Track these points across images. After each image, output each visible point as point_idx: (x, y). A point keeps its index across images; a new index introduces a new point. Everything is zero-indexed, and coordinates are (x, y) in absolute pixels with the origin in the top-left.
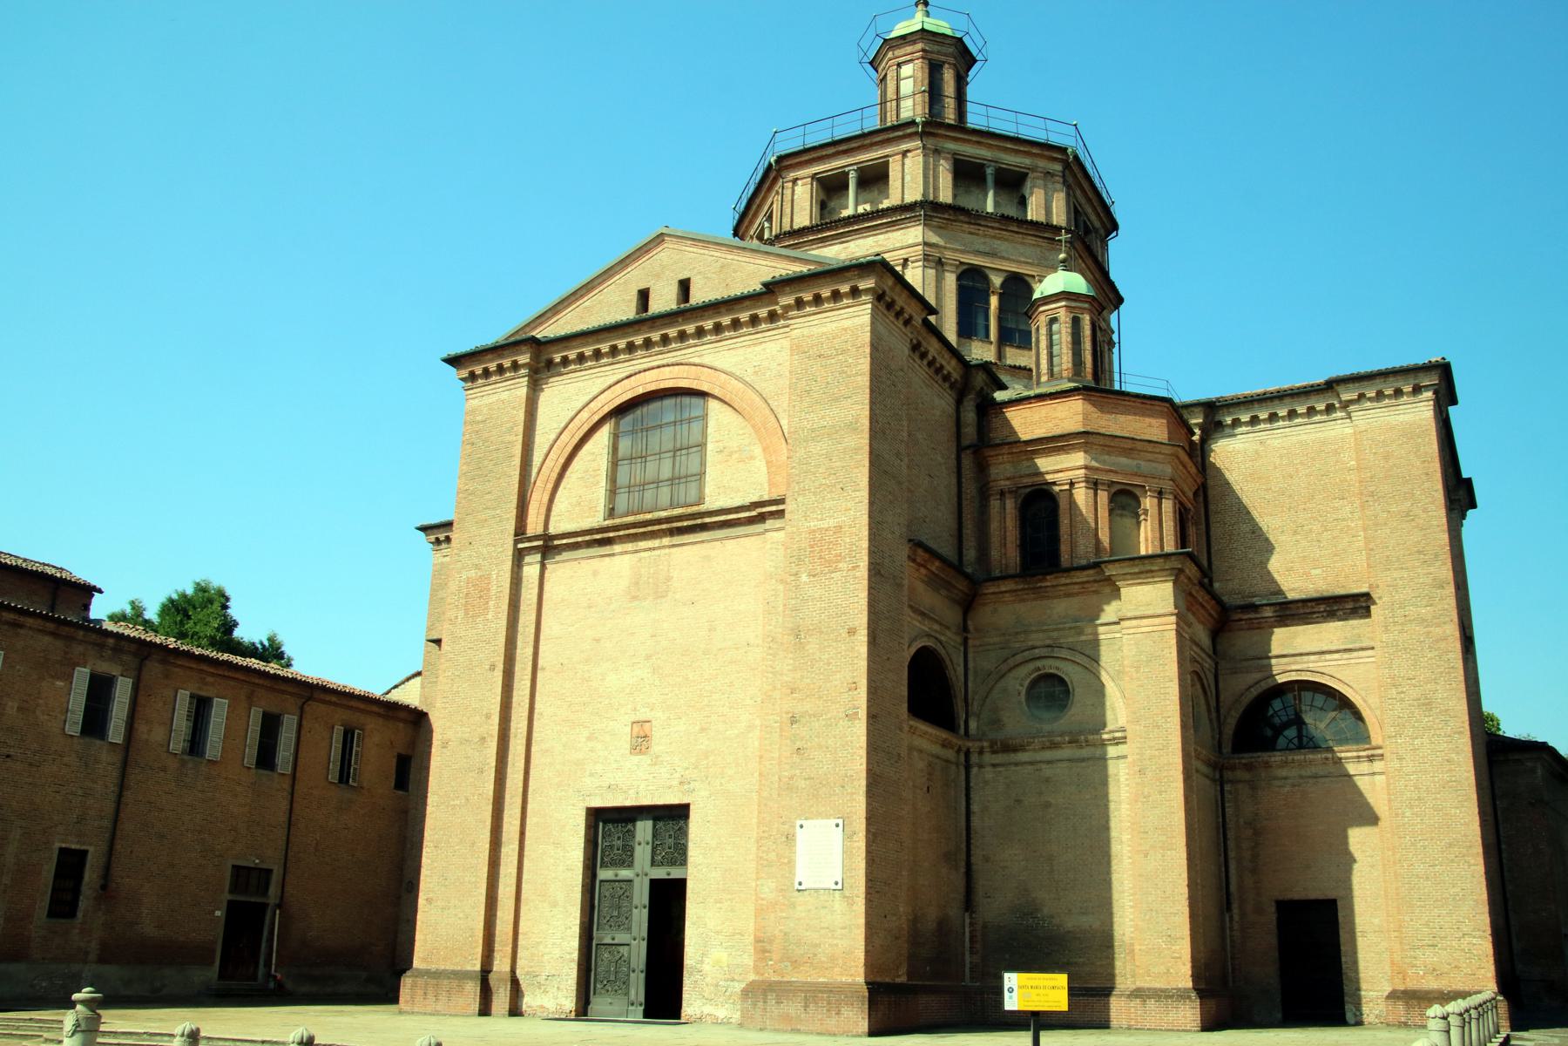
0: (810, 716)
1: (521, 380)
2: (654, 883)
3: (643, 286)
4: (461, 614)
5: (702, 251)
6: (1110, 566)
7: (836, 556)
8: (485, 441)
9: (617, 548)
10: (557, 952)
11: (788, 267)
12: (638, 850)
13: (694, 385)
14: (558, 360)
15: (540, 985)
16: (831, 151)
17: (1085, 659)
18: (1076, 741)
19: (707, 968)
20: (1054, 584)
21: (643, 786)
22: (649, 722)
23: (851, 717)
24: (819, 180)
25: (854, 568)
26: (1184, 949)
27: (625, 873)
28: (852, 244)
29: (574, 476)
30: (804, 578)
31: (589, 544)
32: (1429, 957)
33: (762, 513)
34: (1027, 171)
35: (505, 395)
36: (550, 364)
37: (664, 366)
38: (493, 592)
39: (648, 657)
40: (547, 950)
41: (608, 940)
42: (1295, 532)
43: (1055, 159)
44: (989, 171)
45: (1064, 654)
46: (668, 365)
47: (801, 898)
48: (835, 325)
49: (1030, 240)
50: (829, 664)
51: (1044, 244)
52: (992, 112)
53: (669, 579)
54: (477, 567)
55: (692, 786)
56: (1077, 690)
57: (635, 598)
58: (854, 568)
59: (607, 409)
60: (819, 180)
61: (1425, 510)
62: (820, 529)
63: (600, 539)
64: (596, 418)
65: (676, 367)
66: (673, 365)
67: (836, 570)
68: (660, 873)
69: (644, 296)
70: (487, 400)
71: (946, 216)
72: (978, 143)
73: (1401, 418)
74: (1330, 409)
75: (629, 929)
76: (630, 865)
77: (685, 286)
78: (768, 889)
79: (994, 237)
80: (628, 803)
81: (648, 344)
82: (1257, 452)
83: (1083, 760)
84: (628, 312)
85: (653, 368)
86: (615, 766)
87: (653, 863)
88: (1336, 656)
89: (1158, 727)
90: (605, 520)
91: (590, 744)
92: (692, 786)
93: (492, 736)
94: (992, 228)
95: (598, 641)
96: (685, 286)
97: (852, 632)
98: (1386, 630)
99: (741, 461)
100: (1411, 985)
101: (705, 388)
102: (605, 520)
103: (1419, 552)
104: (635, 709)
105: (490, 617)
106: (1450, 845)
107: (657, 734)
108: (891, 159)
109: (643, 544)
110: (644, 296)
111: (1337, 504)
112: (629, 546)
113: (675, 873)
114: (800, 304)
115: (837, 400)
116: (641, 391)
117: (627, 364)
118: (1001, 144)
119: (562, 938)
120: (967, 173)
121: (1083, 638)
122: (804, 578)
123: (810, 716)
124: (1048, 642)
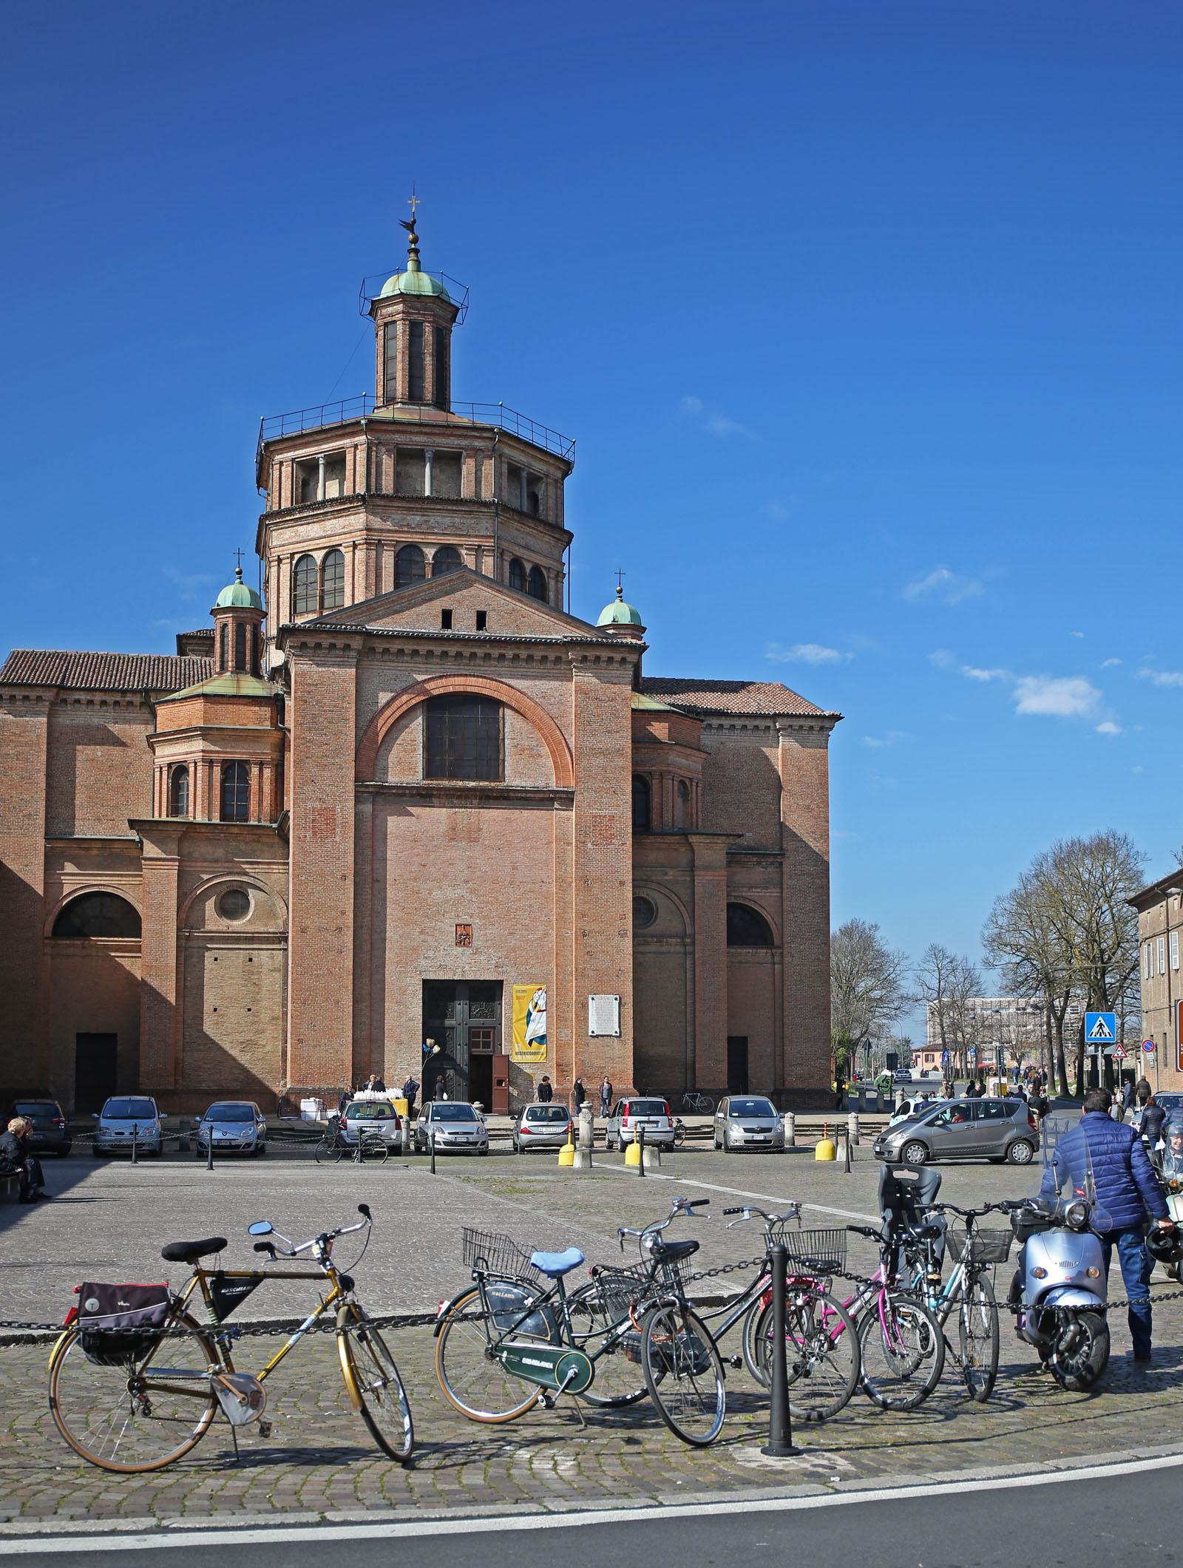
0: (596, 932)
1: (350, 660)
4: (309, 834)
5: (496, 594)
6: (693, 837)
7: (611, 834)
9: (435, 801)
11: (577, 631)
13: (495, 695)
14: (381, 650)
16: (416, 429)
17: (667, 891)
18: (661, 942)
20: (653, 841)
22: (469, 925)
24: (398, 449)
25: (623, 844)
26: (724, 1067)
30: (589, 845)
31: (412, 796)
34: (542, 476)
36: (373, 650)
37: (470, 675)
40: (397, 1073)
42: (738, 807)
43: (559, 468)
44: (524, 474)
45: (654, 886)
46: (474, 676)
47: (593, 1041)
50: (607, 902)
52: (536, 428)
55: (504, 969)
56: (660, 910)
58: (623, 844)
60: (398, 449)
61: (818, 807)
62: (600, 816)
63: (423, 796)
65: (481, 679)
66: (478, 676)
67: (611, 843)
69: (447, 618)
71: (507, 516)
72: (522, 451)
77: (481, 619)
79: (528, 534)
81: (459, 655)
82: (719, 748)
83: (663, 953)
84: (434, 628)
85: (461, 675)
86: (445, 953)
88: (758, 890)
89: (713, 938)
90: (423, 779)
91: (422, 936)
92: (504, 969)
93: (348, 927)
94: (529, 527)
95: (424, 866)
96: (481, 619)
98: (790, 878)
100: (788, 1086)
101: (504, 699)
102: (423, 779)
103: (813, 832)
104: (458, 916)
105: (338, 839)
106: (815, 1008)
108: (464, 453)
110: (447, 618)
111: (765, 792)
113: (488, 1021)
115: (609, 732)
116: (451, 689)
117: (438, 667)
118: (535, 454)
119: (408, 1065)
121: (666, 878)
122: (589, 845)
123: (596, 932)
124: (645, 878)
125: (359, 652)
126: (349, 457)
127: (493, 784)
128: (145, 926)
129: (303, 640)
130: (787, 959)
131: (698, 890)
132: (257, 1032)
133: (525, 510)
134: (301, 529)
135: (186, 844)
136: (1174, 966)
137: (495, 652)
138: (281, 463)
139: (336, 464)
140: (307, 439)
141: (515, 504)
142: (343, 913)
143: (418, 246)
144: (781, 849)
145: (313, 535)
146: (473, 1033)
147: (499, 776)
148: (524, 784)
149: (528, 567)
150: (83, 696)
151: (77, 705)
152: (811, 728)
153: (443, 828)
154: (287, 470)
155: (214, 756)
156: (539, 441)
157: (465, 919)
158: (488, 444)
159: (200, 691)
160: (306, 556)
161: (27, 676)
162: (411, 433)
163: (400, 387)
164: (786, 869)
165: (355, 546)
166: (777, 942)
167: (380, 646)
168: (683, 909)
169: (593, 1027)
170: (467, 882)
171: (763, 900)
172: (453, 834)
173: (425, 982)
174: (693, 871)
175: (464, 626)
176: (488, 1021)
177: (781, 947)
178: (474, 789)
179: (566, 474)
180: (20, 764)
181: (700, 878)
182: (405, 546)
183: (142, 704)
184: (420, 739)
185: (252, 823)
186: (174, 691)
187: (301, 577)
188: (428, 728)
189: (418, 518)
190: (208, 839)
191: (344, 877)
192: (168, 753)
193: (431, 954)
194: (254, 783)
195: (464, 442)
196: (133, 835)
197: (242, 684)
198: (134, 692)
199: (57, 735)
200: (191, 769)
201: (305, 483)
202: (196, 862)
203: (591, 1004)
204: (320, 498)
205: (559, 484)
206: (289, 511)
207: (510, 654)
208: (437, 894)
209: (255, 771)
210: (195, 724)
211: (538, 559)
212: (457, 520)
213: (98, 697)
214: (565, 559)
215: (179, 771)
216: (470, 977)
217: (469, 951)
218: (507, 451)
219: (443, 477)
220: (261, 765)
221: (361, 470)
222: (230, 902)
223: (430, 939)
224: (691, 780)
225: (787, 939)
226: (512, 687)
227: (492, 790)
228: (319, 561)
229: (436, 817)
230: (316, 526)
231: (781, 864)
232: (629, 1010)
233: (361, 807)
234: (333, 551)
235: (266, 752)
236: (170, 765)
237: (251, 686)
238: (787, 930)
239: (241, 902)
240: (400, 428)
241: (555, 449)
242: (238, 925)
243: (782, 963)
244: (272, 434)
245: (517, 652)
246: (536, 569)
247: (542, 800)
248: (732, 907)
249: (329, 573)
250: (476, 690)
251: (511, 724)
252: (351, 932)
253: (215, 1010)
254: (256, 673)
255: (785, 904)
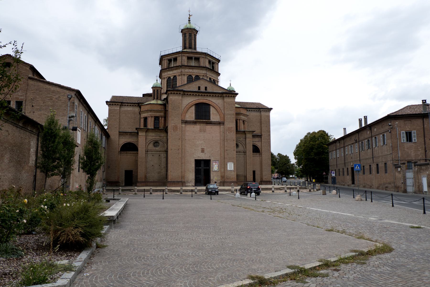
2: (204, 169)
3: (199, 86)
4: (172, 131)
8: (174, 104)
9: (197, 124)
10: (191, 178)
12: (202, 165)
13: (209, 103)
15: (189, 182)
16: (191, 53)
19: (214, 179)
21: (203, 157)
23: (234, 150)
27: (201, 168)
28: (194, 70)
29: (189, 113)
30: (227, 133)
31: (192, 123)
32: (265, 177)
33: (219, 123)
35: (177, 98)
38: (178, 128)
39: (203, 140)
41: (198, 176)
44: (211, 62)
48: (230, 100)
49: (216, 74)
51: (217, 75)
53: (206, 130)
54: (175, 124)
57: (201, 132)
59: (194, 103)
64: (193, 104)
68: (205, 168)
69: (199, 88)
70: (173, 98)
73: (267, 114)
74: (258, 111)
75: (201, 175)
76: (201, 167)
77: (206, 88)
78: (223, 170)
80: (201, 159)
81: (202, 95)
84: (197, 90)
87: (204, 167)
95: (195, 137)
96: (206, 88)
97: (234, 140)
99: (216, 115)
100: (263, 180)
101: (210, 104)
105: (178, 131)
107: (205, 150)
109: (201, 124)
110: (199, 88)
112: (199, 124)
113: (208, 168)
114: (226, 96)
116: (200, 102)
120: (210, 62)
125: (182, 94)
126: (178, 58)
127: (208, 121)
128: (139, 149)
129: (171, 92)
130: (263, 156)
131: (247, 142)
132: (161, 170)
133: (212, 69)
134: (168, 72)
135: (147, 133)
136: (338, 156)
137: (209, 95)
138: (164, 60)
139: (175, 59)
140: (170, 55)
141: (210, 68)
142: (179, 146)
143: (190, 19)
144: (261, 134)
145: (171, 73)
146: (204, 169)
147: (210, 119)
148: (214, 121)
149: (212, 80)
150: (126, 104)
151: (125, 106)
152: (267, 111)
153: (199, 129)
154: (165, 61)
155: (153, 115)
156: (214, 56)
157: (203, 147)
158: (205, 56)
159: (150, 103)
160: (169, 78)
161: (115, 101)
162: (190, 54)
163: (187, 45)
164: (262, 138)
165: (179, 75)
166: (261, 152)
167: (186, 93)
168: (244, 146)
169: (229, 169)
170: (203, 140)
171: (258, 144)
172: (201, 131)
173: (196, 160)
174: (246, 138)
175: (203, 89)
176: (208, 168)
177: (262, 153)
178: (205, 122)
179: (219, 62)
180: (114, 117)
181: (247, 139)
182: (188, 76)
183: (138, 106)
184: (194, 112)
185: (160, 129)
186: (144, 103)
187: (169, 81)
188: (196, 110)
189: (191, 70)
190: (151, 132)
191: (179, 139)
192: (144, 115)
193: (196, 154)
194: (160, 121)
195: (200, 56)
196: (136, 131)
197: (158, 101)
198: (136, 103)
199: (121, 112)
200: (148, 118)
201: (169, 64)
202: (149, 136)
203: (228, 164)
204: (172, 66)
205: (218, 64)
206: (166, 69)
207: (212, 95)
208: (198, 142)
209: (160, 118)
210: (149, 109)
211: (214, 78)
212: (199, 71)
213: (129, 105)
214: (219, 79)
215: (146, 119)
216: (204, 159)
217: (204, 154)
218: (208, 57)
219: (196, 62)
220: (162, 117)
221: (180, 61)
222: (155, 144)
223: (196, 151)
224: (245, 121)
225: (263, 151)
226: (212, 102)
227: (208, 122)
228: (172, 78)
229: (197, 127)
230: (171, 72)
231: (261, 137)
232: (235, 165)
233: (183, 125)
234: (175, 77)
235: (162, 114)
236: (144, 117)
237: (160, 102)
238: (263, 150)
239: (158, 144)
240: (188, 53)
241: (217, 57)
242: (157, 149)
243: (262, 156)
244: (162, 54)
245: (213, 95)
246: (214, 80)
247: (218, 124)
248: (253, 145)
249: (174, 81)
250: (205, 102)
251: (212, 109)
252: (181, 150)
253: (153, 165)
254: (160, 99)
255: (262, 145)
